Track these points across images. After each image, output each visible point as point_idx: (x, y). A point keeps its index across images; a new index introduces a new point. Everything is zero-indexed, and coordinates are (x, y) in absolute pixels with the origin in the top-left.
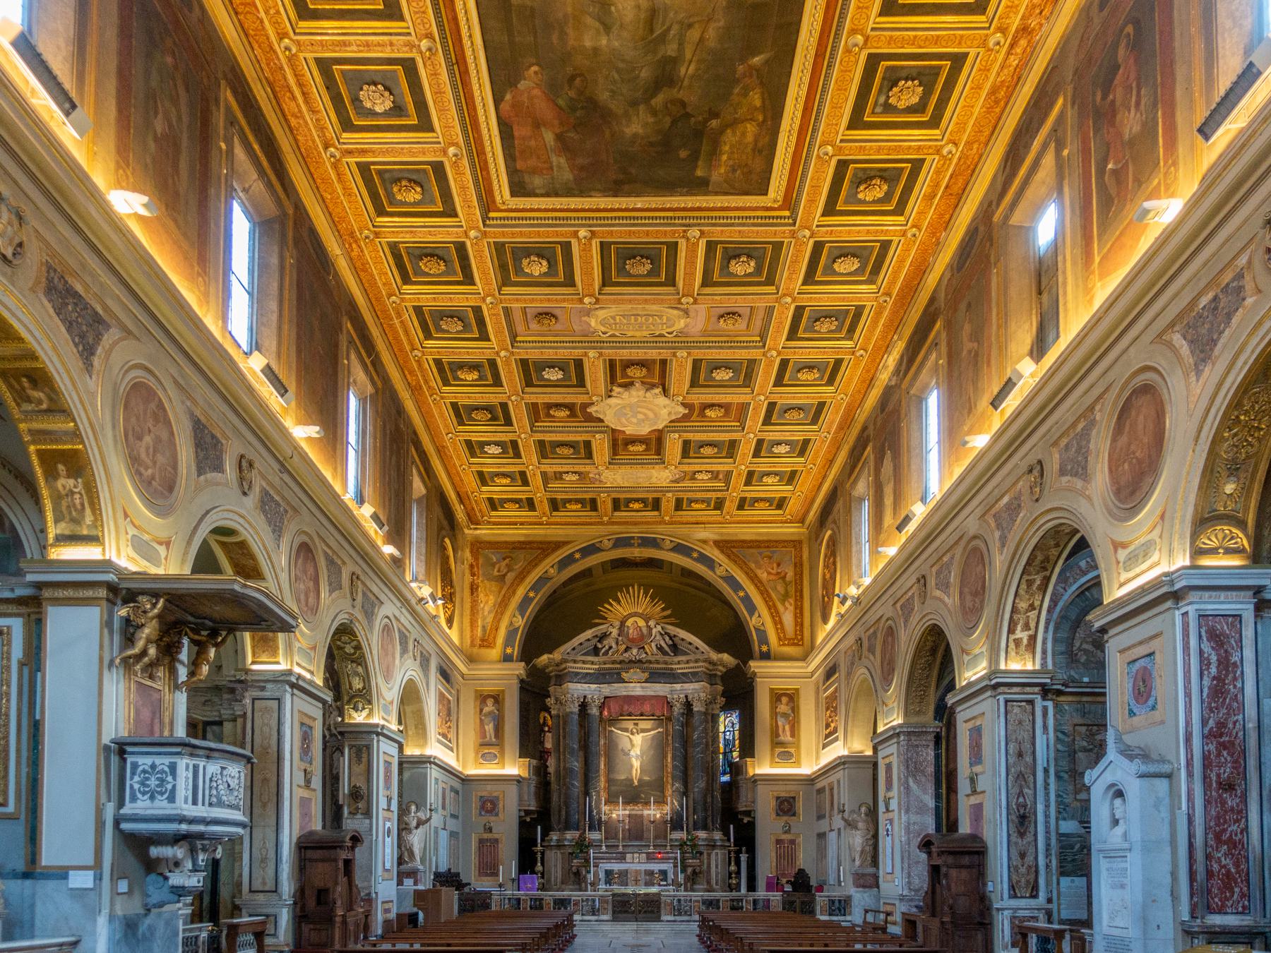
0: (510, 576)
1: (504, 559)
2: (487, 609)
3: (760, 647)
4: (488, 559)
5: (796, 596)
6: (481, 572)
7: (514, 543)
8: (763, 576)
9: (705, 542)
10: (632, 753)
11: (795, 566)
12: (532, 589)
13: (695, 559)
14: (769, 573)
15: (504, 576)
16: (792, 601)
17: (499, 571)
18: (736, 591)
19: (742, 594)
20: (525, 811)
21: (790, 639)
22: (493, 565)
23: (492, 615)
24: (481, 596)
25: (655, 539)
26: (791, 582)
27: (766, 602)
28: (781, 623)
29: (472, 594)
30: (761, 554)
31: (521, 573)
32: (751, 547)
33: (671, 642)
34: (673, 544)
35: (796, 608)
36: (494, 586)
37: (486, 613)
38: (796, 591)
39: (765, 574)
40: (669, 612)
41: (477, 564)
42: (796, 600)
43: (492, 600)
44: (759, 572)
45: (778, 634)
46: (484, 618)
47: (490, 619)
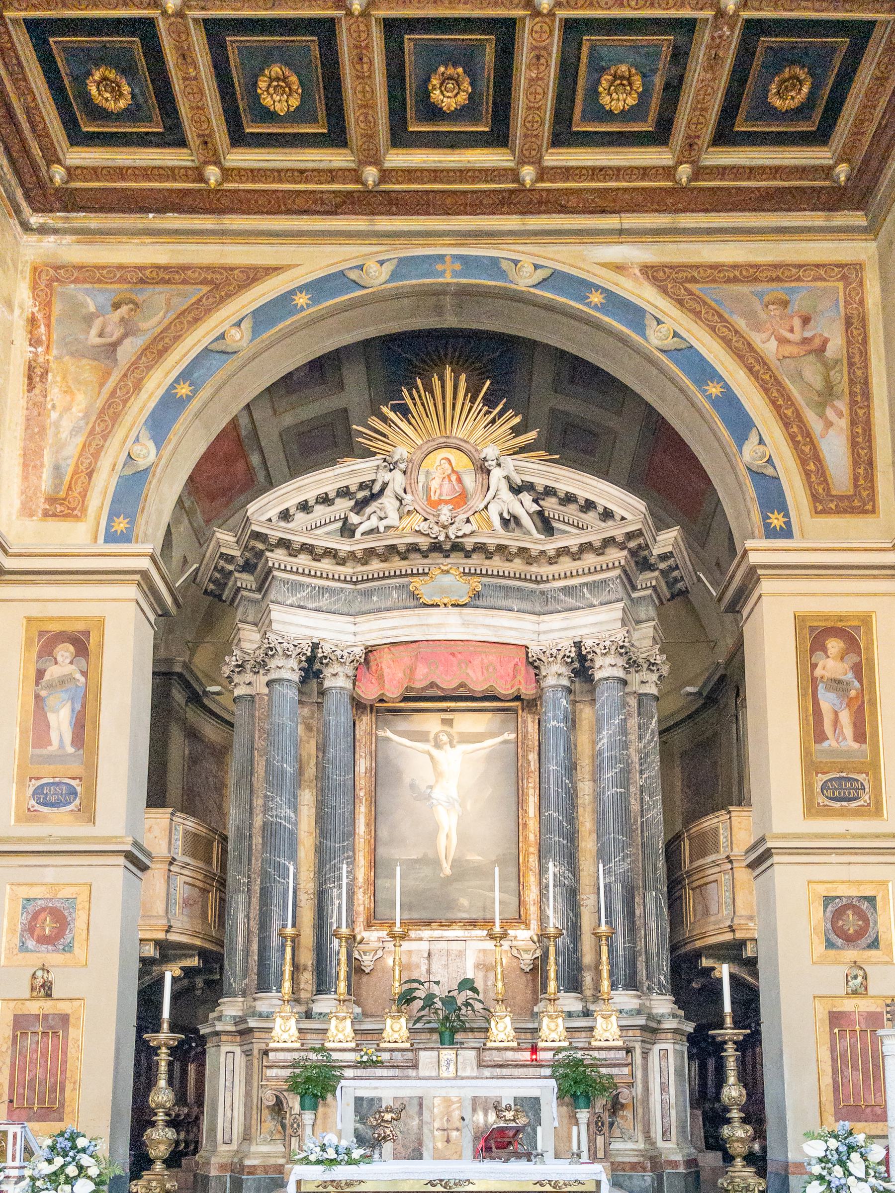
0: (129, 349)
1: (116, 306)
2: (67, 425)
3: (765, 518)
4: (75, 306)
5: (852, 394)
6: (55, 336)
7: (141, 268)
8: (769, 348)
9: (619, 268)
10: (437, 793)
11: (848, 323)
12: (185, 376)
13: (596, 307)
14: (782, 341)
15: (114, 346)
16: (842, 405)
17: (100, 335)
18: (700, 383)
19: (714, 390)
20: (158, 943)
21: (841, 498)
22: (89, 319)
23: (80, 440)
24: (55, 393)
25: (495, 261)
26: (837, 362)
27: (777, 407)
28: (817, 458)
29: (31, 387)
30: (760, 295)
31: (156, 340)
32: (735, 280)
33: (536, 508)
34: (541, 274)
35: (853, 423)
36: (87, 370)
37: (64, 435)
38: (852, 382)
39: (773, 344)
40: (532, 435)
41: (48, 317)
42: (853, 403)
43: (81, 400)
44: (756, 339)
45: (810, 485)
46: (59, 447)
47: (73, 449)
